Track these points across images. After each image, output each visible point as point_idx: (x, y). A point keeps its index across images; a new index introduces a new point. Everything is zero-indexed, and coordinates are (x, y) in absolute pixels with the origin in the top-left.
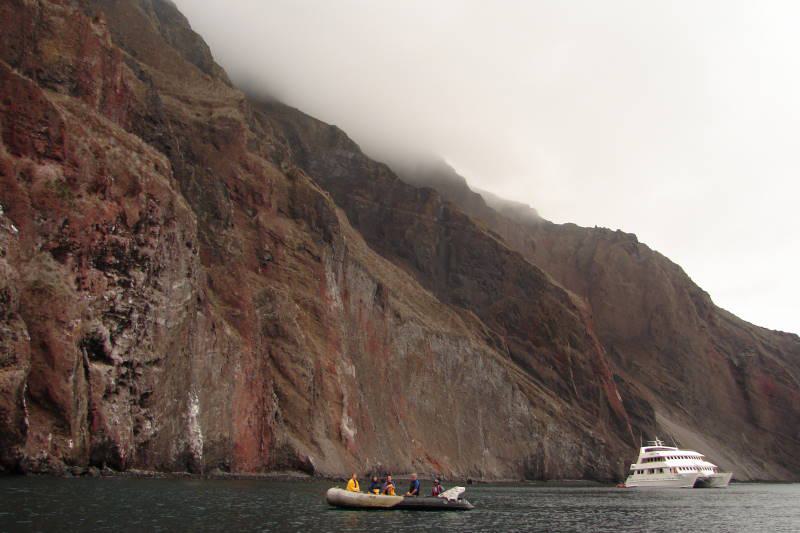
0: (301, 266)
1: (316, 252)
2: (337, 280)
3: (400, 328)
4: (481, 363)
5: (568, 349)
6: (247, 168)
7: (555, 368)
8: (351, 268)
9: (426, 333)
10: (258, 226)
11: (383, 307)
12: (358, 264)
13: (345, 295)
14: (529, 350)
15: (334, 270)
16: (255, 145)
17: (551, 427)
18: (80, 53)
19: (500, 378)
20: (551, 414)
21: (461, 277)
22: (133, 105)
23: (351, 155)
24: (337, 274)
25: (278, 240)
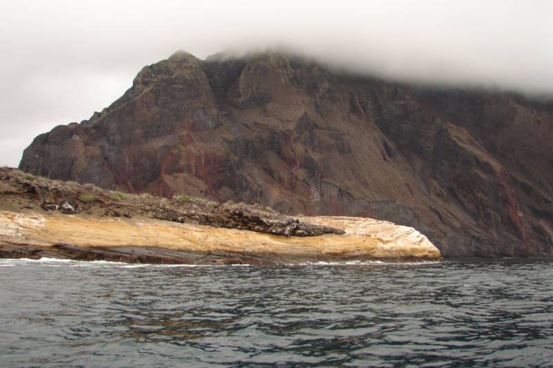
3: (353, 203)
4: (401, 210)
5: (480, 195)
6: (293, 150)
7: (474, 204)
8: (323, 185)
9: (369, 202)
10: (292, 174)
12: (327, 183)
13: (322, 195)
14: (466, 196)
15: (316, 187)
16: (296, 140)
17: (451, 234)
18: (188, 161)
19: (412, 216)
20: (453, 228)
21: (444, 161)
23: (402, 103)
24: (317, 188)
25: (297, 179)
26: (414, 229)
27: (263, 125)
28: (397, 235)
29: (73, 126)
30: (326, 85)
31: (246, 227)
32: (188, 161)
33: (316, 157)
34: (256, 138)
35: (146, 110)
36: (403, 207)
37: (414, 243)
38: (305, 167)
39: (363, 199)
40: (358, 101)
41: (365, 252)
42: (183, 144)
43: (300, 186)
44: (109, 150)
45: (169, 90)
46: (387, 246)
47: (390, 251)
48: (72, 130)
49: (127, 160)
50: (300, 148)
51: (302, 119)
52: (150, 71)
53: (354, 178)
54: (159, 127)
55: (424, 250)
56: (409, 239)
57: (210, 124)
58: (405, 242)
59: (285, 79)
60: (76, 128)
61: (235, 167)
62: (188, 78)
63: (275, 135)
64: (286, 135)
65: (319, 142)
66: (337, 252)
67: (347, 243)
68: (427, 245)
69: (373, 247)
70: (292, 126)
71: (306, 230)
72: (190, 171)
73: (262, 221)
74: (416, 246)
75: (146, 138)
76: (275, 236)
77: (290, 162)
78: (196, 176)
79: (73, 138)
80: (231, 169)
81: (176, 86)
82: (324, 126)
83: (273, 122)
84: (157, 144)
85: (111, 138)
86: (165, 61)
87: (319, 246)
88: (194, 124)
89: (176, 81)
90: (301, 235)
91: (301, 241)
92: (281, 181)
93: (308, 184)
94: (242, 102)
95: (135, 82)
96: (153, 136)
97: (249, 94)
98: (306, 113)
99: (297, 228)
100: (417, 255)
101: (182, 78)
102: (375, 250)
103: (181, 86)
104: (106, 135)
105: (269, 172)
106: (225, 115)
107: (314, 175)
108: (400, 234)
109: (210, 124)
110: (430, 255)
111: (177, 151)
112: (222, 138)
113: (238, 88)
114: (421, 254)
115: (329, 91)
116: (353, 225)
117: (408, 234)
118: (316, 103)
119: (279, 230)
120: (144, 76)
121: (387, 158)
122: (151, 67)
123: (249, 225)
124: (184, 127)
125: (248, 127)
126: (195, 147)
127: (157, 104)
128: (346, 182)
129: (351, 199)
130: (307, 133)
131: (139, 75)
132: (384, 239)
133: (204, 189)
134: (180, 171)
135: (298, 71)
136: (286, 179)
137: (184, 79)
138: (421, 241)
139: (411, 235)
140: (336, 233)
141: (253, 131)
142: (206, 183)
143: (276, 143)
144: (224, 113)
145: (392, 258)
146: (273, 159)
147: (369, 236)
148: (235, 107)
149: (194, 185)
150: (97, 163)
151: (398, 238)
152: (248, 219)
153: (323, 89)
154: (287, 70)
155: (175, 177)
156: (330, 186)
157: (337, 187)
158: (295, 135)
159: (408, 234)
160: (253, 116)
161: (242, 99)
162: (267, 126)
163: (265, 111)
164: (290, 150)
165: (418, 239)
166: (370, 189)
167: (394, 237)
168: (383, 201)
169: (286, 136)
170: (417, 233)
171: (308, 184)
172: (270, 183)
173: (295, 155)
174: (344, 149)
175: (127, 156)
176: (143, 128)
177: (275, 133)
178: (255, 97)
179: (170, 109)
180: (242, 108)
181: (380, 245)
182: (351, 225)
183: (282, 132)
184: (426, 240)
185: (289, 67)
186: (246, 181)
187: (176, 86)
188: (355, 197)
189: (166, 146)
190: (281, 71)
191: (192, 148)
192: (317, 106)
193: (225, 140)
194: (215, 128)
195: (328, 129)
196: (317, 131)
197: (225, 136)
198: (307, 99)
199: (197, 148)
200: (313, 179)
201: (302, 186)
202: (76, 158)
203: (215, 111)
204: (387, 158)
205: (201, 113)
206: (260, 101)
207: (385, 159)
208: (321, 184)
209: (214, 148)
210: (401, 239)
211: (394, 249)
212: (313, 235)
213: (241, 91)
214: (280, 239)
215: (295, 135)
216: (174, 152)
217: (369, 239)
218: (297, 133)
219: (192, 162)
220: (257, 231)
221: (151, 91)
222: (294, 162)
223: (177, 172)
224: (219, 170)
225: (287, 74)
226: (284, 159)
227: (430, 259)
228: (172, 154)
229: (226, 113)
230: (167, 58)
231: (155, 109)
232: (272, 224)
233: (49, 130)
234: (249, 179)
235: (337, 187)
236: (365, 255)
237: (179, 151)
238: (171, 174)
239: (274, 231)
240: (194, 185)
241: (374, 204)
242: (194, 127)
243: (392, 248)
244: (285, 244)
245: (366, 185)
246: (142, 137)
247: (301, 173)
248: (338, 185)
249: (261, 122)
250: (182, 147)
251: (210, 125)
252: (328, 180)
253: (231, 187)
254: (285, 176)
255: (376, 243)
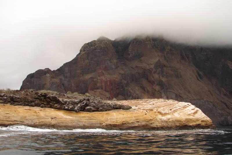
0: (158, 94)
1: (160, 92)
2: (165, 95)
4: (207, 103)
6: (153, 77)
8: (168, 93)
10: (153, 88)
11: (177, 97)
12: (170, 91)
15: (165, 94)
16: (154, 73)
18: (101, 84)
22: (117, 82)
25: (155, 90)
26: (190, 104)
27: (140, 67)
28: (175, 109)
29: (47, 70)
30: (169, 47)
31: (49, 106)
32: (101, 84)
33: (164, 80)
34: (136, 73)
35: (83, 62)
36: (208, 101)
37: (189, 115)
38: (159, 85)
39: (187, 98)
40: (184, 54)
41: (144, 123)
42: (99, 76)
43: (157, 94)
44: (65, 80)
45: (94, 52)
46: (164, 118)
47: (166, 122)
48: (46, 71)
49: (73, 85)
50: (156, 76)
51: (157, 63)
52: (87, 45)
53: (183, 89)
54: (89, 69)
55: (197, 120)
56: (186, 111)
57: (113, 67)
58: (181, 114)
59: (150, 46)
60: (48, 71)
61: (125, 86)
62: (102, 46)
63: (145, 71)
64: (150, 70)
65: (166, 73)
66: (117, 124)
67: (129, 116)
68: (201, 116)
69: (151, 118)
70: (152, 66)
71: (94, 107)
72: (102, 88)
73: (59, 100)
74: (191, 117)
75: (83, 75)
76: (68, 112)
77: (152, 83)
78: (105, 90)
79: (47, 75)
80: (123, 87)
81: (97, 50)
82: (169, 66)
83: (144, 65)
84: (88, 77)
85: (65, 75)
86: (95, 41)
87: (103, 119)
88: (105, 67)
89: (97, 48)
90: (89, 111)
91: (88, 115)
92: (148, 92)
93: (161, 93)
94: (131, 57)
95: (81, 51)
96: (86, 74)
97: (134, 54)
98: (159, 60)
99: (87, 105)
100: (191, 124)
101: (100, 46)
102: (153, 122)
103: (99, 50)
104: (63, 74)
105: (143, 88)
106: (123, 64)
107: (163, 88)
108: (178, 108)
109: (113, 67)
110: (203, 124)
111: (96, 79)
112: (119, 73)
113: (128, 51)
114: (194, 124)
115: (171, 50)
116: (145, 103)
117: (185, 107)
118: (165, 56)
119: (71, 107)
120: (84, 47)
121: (199, 79)
122: (88, 44)
123: (51, 104)
124: (101, 69)
125: (133, 68)
126: (105, 77)
127: (88, 59)
128: (179, 91)
129: (182, 99)
130: (160, 69)
131: (82, 47)
132: (163, 112)
133: (108, 97)
134: (98, 88)
135: (156, 42)
136: (150, 91)
137: (100, 47)
138: (196, 112)
139: (187, 108)
140: (123, 109)
141: (135, 70)
142: (110, 94)
143: (145, 75)
144: (122, 63)
145: (168, 127)
146: (144, 82)
147: (152, 110)
148: (127, 60)
149: (103, 95)
150: (55, 86)
151: (175, 111)
152: (51, 100)
153: (168, 49)
154: (151, 42)
155: (95, 92)
156: (171, 93)
157: (175, 93)
158: (154, 70)
159: (185, 107)
160: (135, 63)
161: (130, 56)
162: (142, 67)
163: (141, 60)
164: (152, 77)
165: (193, 111)
166: (191, 94)
167: (172, 110)
168: (197, 99)
169: (150, 71)
170: (193, 107)
171: (161, 93)
172: (143, 93)
173: (154, 79)
174: (178, 76)
175: (73, 83)
176: (81, 70)
177: (145, 70)
178: (136, 55)
179: (94, 61)
180: (130, 60)
181: (160, 117)
182: (143, 103)
183: (148, 69)
184: (200, 111)
185: (152, 41)
186: (130, 92)
187: (97, 50)
188: (184, 98)
189: (91, 78)
190: (148, 42)
191: (103, 78)
192: (165, 57)
193: (120, 74)
194: (116, 69)
195: (170, 67)
196: (165, 68)
197: (120, 72)
198: (160, 54)
199: (106, 77)
200: (163, 90)
201: (158, 93)
202: (45, 84)
203: (115, 61)
204: (199, 79)
205: (109, 62)
206: (139, 57)
207: (198, 79)
208: (167, 92)
209: (114, 78)
210: (178, 112)
211: (171, 120)
212: (101, 111)
213: (130, 52)
214: (72, 114)
215: (154, 70)
216: (95, 80)
217: (151, 112)
218: (155, 69)
219: (103, 84)
220: (56, 108)
221: (85, 53)
222: (154, 83)
223: (96, 89)
224: (117, 87)
225: (150, 44)
226: (150, 82)
227: (203, 127)
228: (93, 81)
229: (123, 63)
230: (96, 39)
231: (87, 61)
232: (66, 102)
233: (34, 72)
234: (131, 91)
235: (175, 93)
236: (143, 126)
237: (97, 79)
238: (93, 90)
239: (66, 108)
240: (103, 95)
241: (193, 100)
242: (106, 69)
243: (169, 119)
244: (74, 118)
245: (189, 92)
246: (80, 74)
247: (157, 88)
248: (175, 92)
249: (139, 66)
250: (98, 77)
251: (113, 67)
252: (170, 90)
253: (123, 95)
254: (150, 89)
255: (157, 115)
